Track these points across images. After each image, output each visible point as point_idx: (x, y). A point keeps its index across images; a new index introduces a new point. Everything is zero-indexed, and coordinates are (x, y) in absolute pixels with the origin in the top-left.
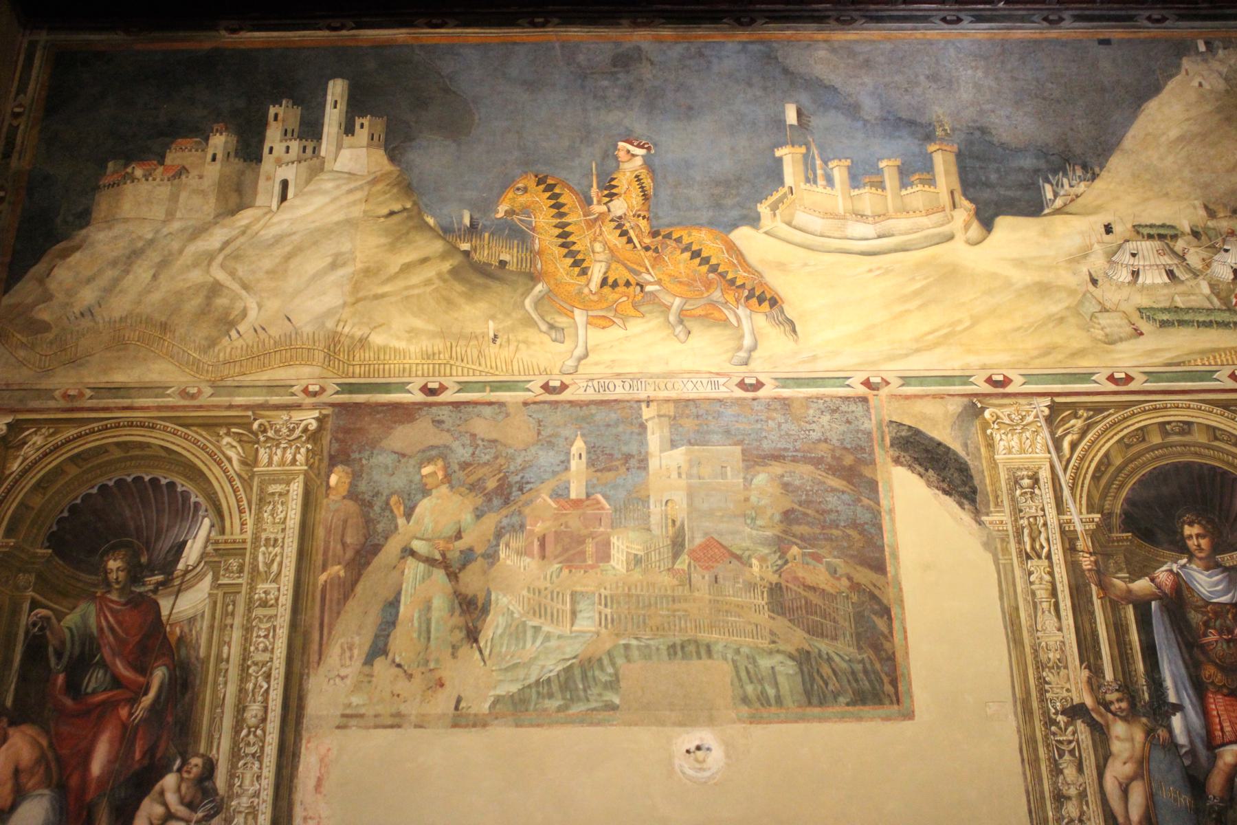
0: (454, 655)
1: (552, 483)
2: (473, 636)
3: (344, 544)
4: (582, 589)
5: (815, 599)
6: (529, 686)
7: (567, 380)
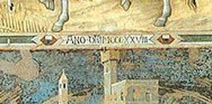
7: (56, 35)
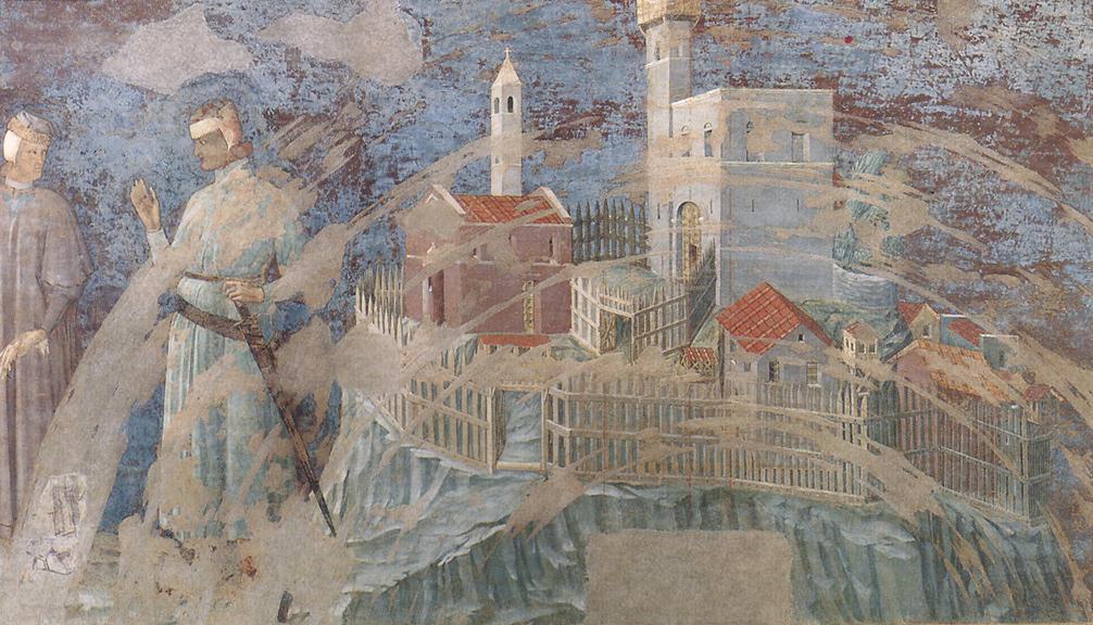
0: (273, 516)
1: (453, 163)
2: (307, 476)
3: (44, 289)
4: (519, 387)
5: (959, 415)
6: (418, 576)
